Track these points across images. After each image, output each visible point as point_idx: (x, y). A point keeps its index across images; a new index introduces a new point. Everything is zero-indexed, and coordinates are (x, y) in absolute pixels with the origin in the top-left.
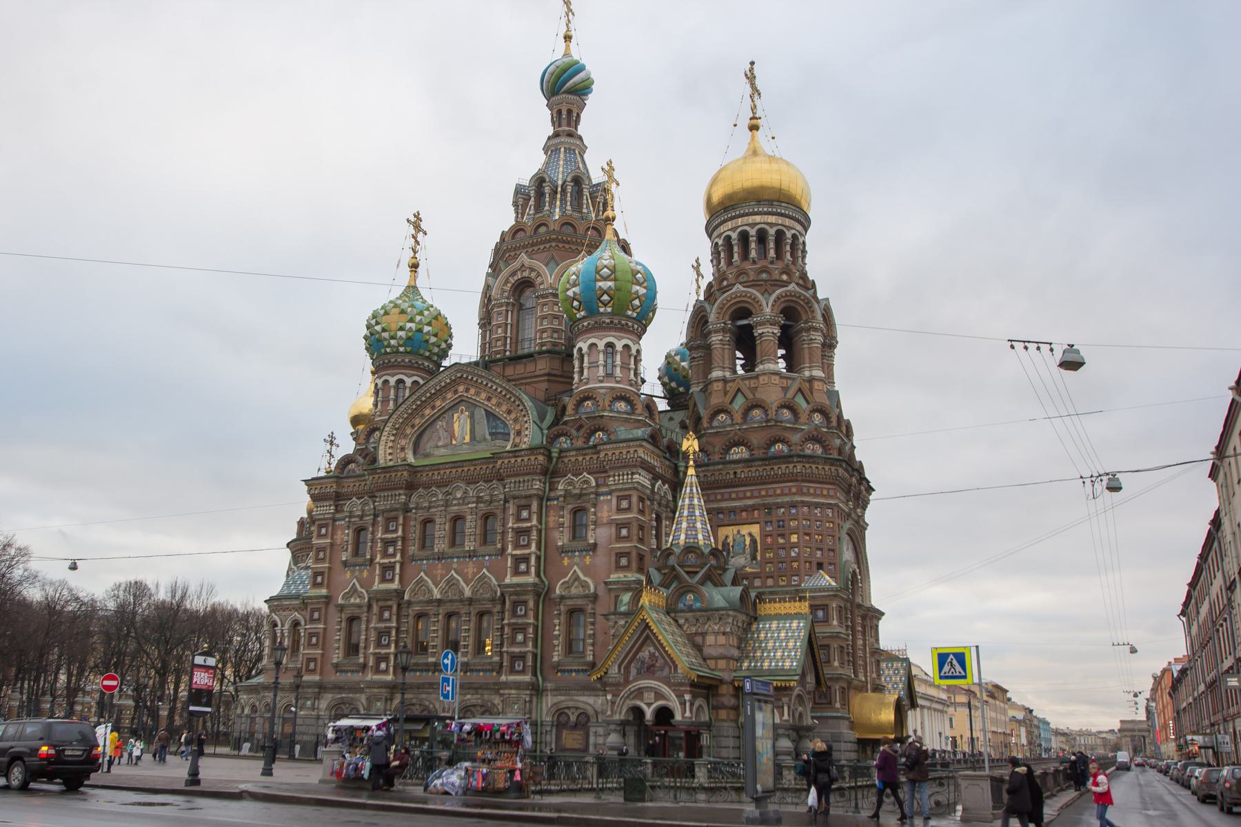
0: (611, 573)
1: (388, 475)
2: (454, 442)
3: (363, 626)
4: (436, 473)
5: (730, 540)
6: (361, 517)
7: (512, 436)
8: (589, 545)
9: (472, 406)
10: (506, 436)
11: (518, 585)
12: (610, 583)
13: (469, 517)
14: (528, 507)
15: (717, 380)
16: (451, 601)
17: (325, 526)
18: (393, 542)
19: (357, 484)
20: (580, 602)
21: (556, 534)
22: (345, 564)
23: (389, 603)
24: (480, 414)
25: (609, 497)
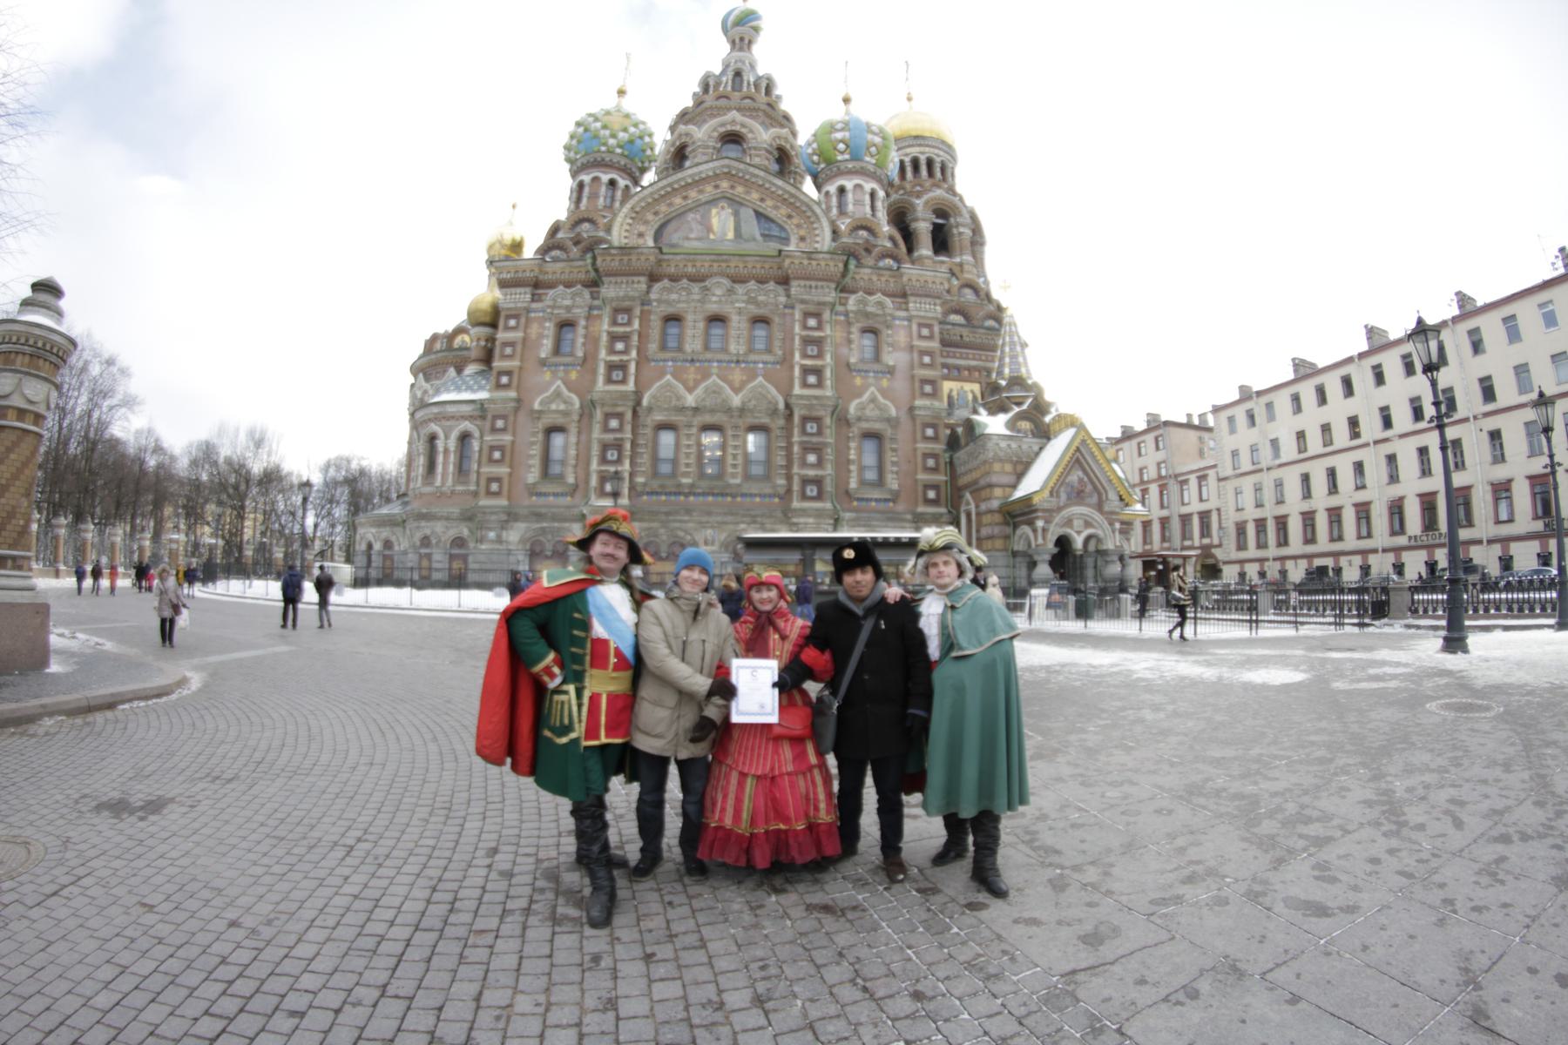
0: (914, 398)
1: (626, 258)
2: (712, 237)
3: (573, 439)
4: (690, 264)
5: (954, 394)
6: (568, 309)
7: (794, 239)
8: (888, 366)
9: (735, 203)
10: (786, 240)
11: (816, 398)
12: (920, 408)
13: (735, 318)
14: (817, 315)
15: (927, 257)
16: (712, 411)
17: (516, 317)
18: (625, 338)
19: (567, 271)
20: (877, 426)
21: (844, 351)
22: (543, 363)
23: (619, 409)
24: (747, 214)
25: (906, 323)
